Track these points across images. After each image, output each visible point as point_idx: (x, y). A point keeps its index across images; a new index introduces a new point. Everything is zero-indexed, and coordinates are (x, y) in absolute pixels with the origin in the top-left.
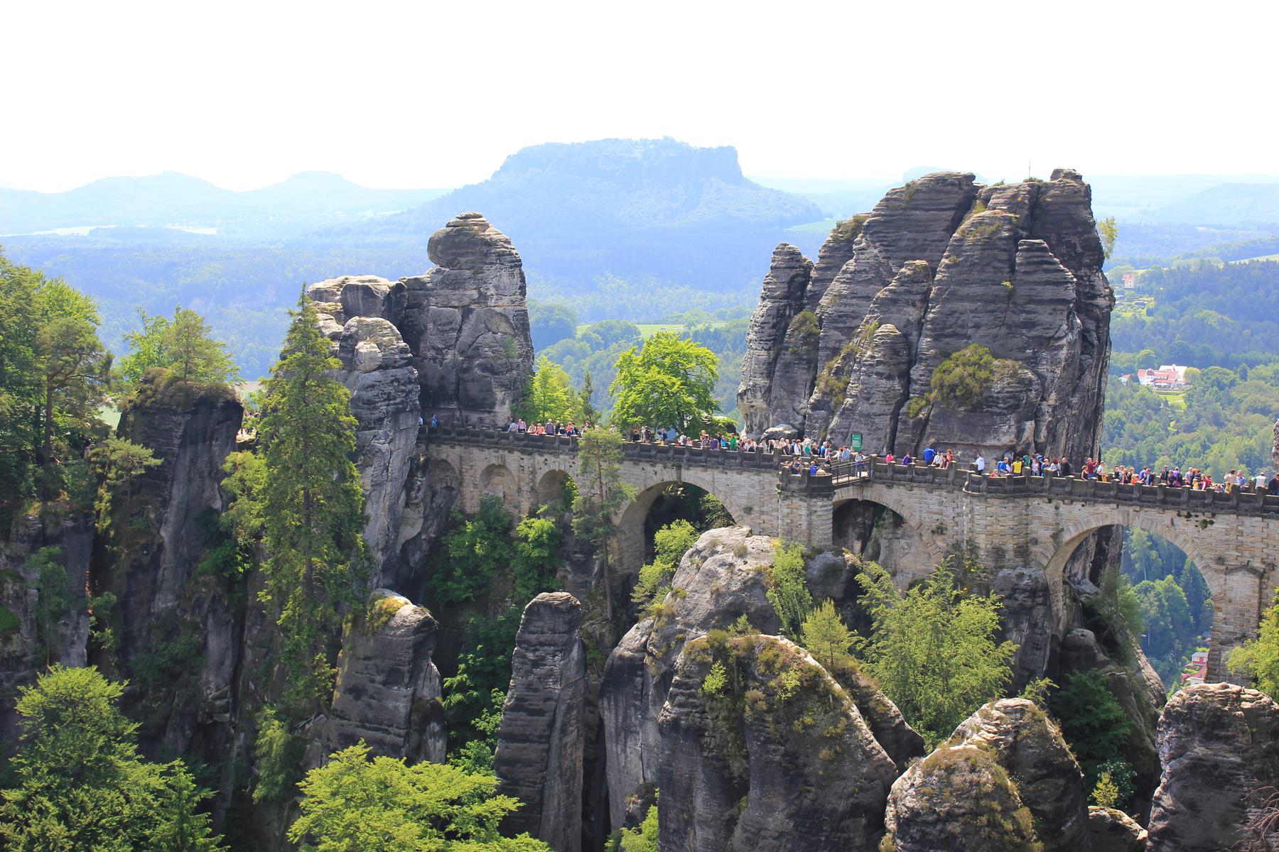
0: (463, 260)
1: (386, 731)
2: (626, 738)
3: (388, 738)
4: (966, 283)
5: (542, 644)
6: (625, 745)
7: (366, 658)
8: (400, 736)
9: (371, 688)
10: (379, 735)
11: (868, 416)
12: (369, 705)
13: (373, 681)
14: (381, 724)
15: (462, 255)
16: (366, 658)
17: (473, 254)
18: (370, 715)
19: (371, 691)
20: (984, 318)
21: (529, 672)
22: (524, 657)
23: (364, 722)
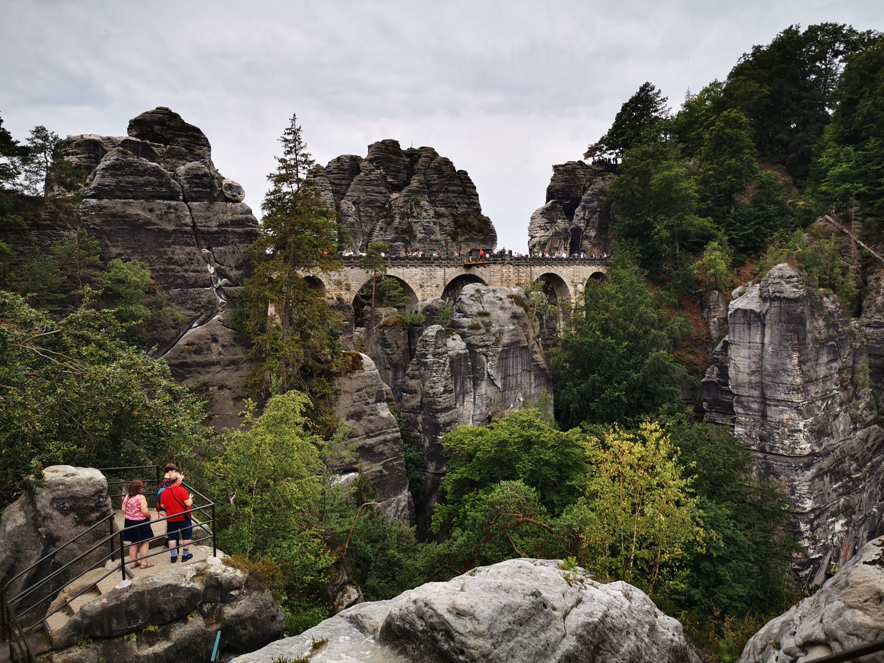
0: (180, 139)
1: (383, 434)
2: (464, 398)
3: (389, 437)
4: (449, 185)
5: (444, 353)
6: (463, 401)
7: (358, 390)
8: (397, 431)
9: (367, 409)
10: (382, 438)
11: (437, 241)
12: (370, 421)
13: (368, 404)
14: (382, 429)
15: (179, 136)
16: (358, 390)
17: (187, 136)
18: (372, 426)
19: (368, 410)
20: (460, 201)
21: (443, 370)
22: (438, 362)
23: (368, 434)
